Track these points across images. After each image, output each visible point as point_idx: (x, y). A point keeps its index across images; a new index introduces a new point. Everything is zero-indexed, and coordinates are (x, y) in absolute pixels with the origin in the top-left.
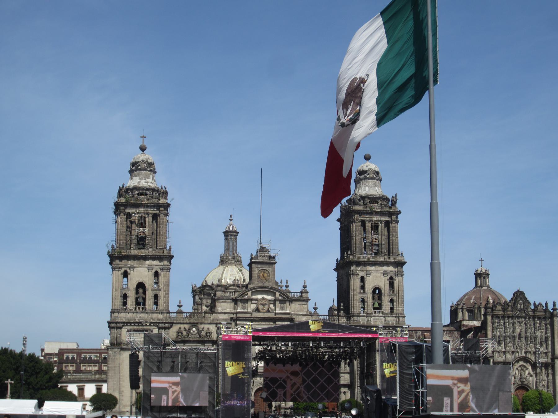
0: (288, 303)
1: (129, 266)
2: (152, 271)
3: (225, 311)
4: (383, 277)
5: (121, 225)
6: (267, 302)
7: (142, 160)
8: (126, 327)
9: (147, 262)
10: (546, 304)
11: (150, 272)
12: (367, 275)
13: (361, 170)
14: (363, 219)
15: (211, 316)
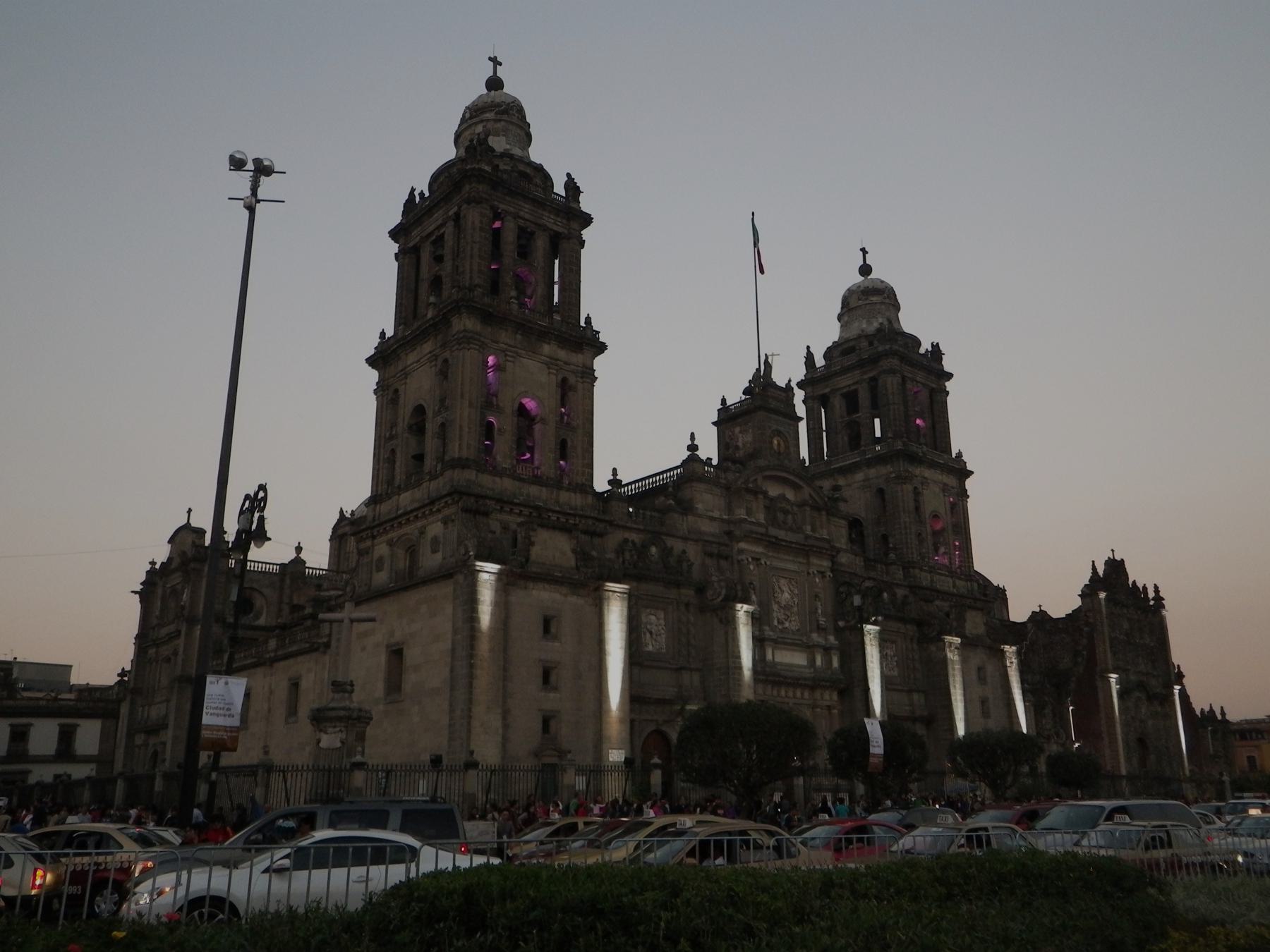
0: (824, 518)
1: (505, 347)
2: (557, 376)
3: (711, 514)
4: (941, 495)
5: (483, 234)
6: (789, 507)
7: (513, 102)
8: (499, 516)
9: (546, 349)
10: (1145, 588)
11: (553, 377)
12: (922, 484)
13: (870, 287)
14: (906, 374)
15: (683, 521)
